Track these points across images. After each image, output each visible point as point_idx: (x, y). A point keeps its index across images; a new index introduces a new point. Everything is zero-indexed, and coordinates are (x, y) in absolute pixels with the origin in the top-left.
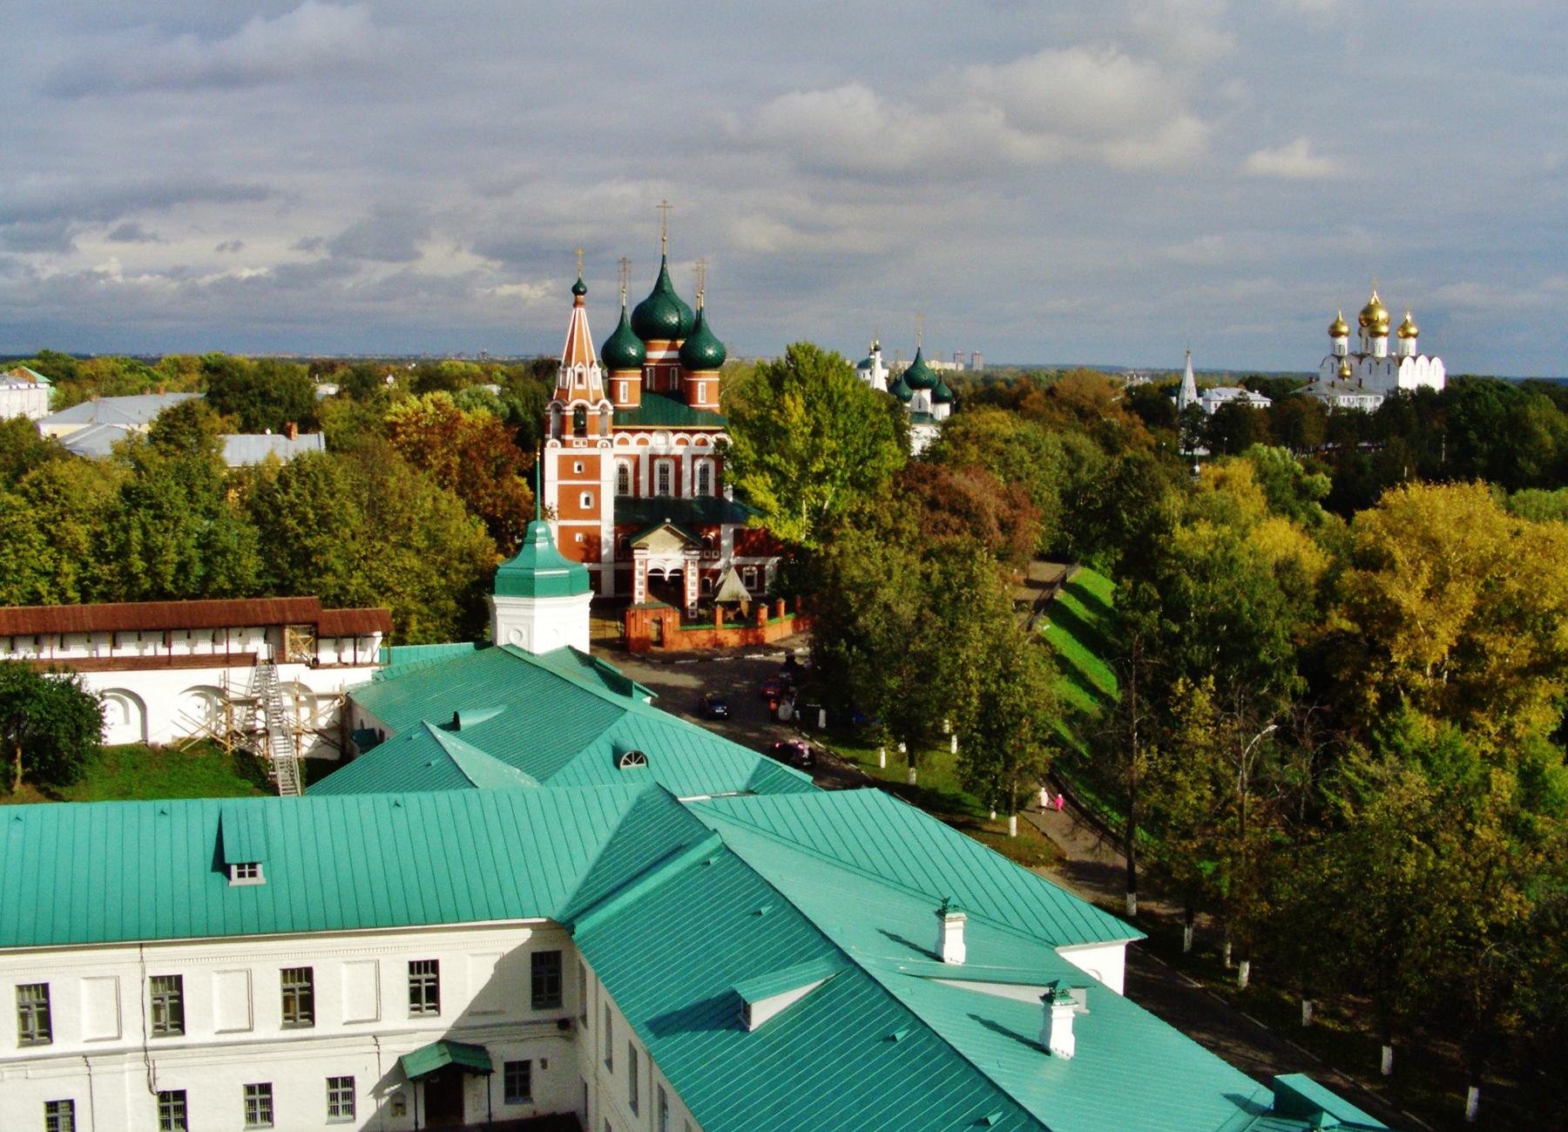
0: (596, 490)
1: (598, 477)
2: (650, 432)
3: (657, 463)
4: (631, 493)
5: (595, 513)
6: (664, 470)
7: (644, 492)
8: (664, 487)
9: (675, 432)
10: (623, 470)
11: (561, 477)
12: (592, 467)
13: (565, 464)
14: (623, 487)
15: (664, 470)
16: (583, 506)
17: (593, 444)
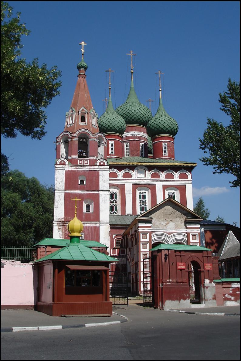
0: (96, 199)
1: (97, 188)
2: (132, 168)
3: (138, 193)
4: (119, 213)
5: (96, 217)
6: (143, 197)
9: (150, 168)
10: (113, 196)
11: (66, 189)
12: (93, 180)
13: (71, 180)
14: (113, 209)
15: (143, 197)
16: (85, 210)
17: (93, 163)
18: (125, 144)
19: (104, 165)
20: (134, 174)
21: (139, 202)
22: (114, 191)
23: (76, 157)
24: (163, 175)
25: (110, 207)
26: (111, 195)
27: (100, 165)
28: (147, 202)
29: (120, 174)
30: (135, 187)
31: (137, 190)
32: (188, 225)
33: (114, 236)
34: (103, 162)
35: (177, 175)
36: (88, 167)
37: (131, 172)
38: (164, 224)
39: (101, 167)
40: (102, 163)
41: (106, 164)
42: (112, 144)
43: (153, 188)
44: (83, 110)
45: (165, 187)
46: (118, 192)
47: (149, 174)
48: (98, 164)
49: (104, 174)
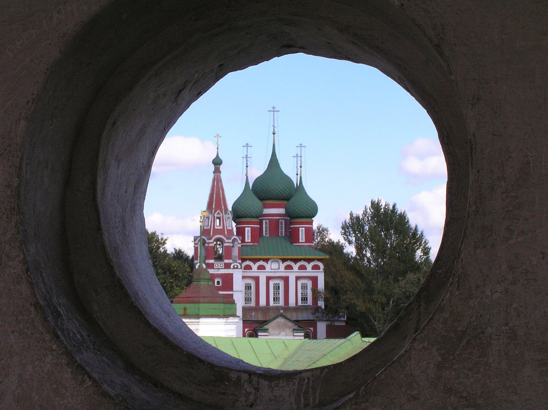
1: (231, 289)
2: (267, 260)
3: (272, 283)
4: (253, 304)
6: (277, 287)
7: (263, 302)
8: (276, 299)
9: (284, 260)
10: (248, 287)
14: (248, 300)
17: (227, 266)
18: (264, 222)
19: (237, 268)
20: (268, 266)
21: (273, 292)
22: (249, 283)
23: (212, 261)
24: (296, 267)
25: (246, 298)
26: (246, 287)
27: (234, 268)
28: (280, 293)
29: (255, 267)
30: (268, 279)
31: (270, 282)
32: (295, 334)
33: (246, 330)
34: (237, 266)
35: (309, 266)
36: (224, 270)
37: (264, 263)
38: (277, 333)
39: (235, 270)
40: (236, 267)
41: (239, 267)
42: (249, 231)
43: (286, 280)
44: (219, 213)
45: (297, 278)
46: (252, 283)
47: (283, 266)
48: (232, 267)
49: (238, 276)
